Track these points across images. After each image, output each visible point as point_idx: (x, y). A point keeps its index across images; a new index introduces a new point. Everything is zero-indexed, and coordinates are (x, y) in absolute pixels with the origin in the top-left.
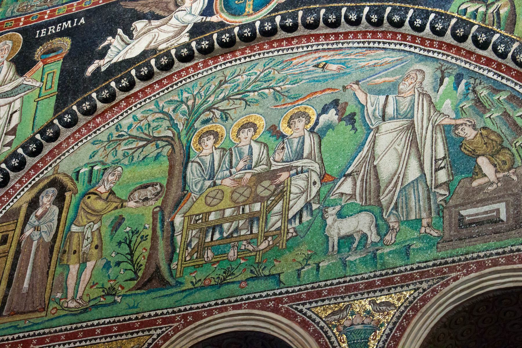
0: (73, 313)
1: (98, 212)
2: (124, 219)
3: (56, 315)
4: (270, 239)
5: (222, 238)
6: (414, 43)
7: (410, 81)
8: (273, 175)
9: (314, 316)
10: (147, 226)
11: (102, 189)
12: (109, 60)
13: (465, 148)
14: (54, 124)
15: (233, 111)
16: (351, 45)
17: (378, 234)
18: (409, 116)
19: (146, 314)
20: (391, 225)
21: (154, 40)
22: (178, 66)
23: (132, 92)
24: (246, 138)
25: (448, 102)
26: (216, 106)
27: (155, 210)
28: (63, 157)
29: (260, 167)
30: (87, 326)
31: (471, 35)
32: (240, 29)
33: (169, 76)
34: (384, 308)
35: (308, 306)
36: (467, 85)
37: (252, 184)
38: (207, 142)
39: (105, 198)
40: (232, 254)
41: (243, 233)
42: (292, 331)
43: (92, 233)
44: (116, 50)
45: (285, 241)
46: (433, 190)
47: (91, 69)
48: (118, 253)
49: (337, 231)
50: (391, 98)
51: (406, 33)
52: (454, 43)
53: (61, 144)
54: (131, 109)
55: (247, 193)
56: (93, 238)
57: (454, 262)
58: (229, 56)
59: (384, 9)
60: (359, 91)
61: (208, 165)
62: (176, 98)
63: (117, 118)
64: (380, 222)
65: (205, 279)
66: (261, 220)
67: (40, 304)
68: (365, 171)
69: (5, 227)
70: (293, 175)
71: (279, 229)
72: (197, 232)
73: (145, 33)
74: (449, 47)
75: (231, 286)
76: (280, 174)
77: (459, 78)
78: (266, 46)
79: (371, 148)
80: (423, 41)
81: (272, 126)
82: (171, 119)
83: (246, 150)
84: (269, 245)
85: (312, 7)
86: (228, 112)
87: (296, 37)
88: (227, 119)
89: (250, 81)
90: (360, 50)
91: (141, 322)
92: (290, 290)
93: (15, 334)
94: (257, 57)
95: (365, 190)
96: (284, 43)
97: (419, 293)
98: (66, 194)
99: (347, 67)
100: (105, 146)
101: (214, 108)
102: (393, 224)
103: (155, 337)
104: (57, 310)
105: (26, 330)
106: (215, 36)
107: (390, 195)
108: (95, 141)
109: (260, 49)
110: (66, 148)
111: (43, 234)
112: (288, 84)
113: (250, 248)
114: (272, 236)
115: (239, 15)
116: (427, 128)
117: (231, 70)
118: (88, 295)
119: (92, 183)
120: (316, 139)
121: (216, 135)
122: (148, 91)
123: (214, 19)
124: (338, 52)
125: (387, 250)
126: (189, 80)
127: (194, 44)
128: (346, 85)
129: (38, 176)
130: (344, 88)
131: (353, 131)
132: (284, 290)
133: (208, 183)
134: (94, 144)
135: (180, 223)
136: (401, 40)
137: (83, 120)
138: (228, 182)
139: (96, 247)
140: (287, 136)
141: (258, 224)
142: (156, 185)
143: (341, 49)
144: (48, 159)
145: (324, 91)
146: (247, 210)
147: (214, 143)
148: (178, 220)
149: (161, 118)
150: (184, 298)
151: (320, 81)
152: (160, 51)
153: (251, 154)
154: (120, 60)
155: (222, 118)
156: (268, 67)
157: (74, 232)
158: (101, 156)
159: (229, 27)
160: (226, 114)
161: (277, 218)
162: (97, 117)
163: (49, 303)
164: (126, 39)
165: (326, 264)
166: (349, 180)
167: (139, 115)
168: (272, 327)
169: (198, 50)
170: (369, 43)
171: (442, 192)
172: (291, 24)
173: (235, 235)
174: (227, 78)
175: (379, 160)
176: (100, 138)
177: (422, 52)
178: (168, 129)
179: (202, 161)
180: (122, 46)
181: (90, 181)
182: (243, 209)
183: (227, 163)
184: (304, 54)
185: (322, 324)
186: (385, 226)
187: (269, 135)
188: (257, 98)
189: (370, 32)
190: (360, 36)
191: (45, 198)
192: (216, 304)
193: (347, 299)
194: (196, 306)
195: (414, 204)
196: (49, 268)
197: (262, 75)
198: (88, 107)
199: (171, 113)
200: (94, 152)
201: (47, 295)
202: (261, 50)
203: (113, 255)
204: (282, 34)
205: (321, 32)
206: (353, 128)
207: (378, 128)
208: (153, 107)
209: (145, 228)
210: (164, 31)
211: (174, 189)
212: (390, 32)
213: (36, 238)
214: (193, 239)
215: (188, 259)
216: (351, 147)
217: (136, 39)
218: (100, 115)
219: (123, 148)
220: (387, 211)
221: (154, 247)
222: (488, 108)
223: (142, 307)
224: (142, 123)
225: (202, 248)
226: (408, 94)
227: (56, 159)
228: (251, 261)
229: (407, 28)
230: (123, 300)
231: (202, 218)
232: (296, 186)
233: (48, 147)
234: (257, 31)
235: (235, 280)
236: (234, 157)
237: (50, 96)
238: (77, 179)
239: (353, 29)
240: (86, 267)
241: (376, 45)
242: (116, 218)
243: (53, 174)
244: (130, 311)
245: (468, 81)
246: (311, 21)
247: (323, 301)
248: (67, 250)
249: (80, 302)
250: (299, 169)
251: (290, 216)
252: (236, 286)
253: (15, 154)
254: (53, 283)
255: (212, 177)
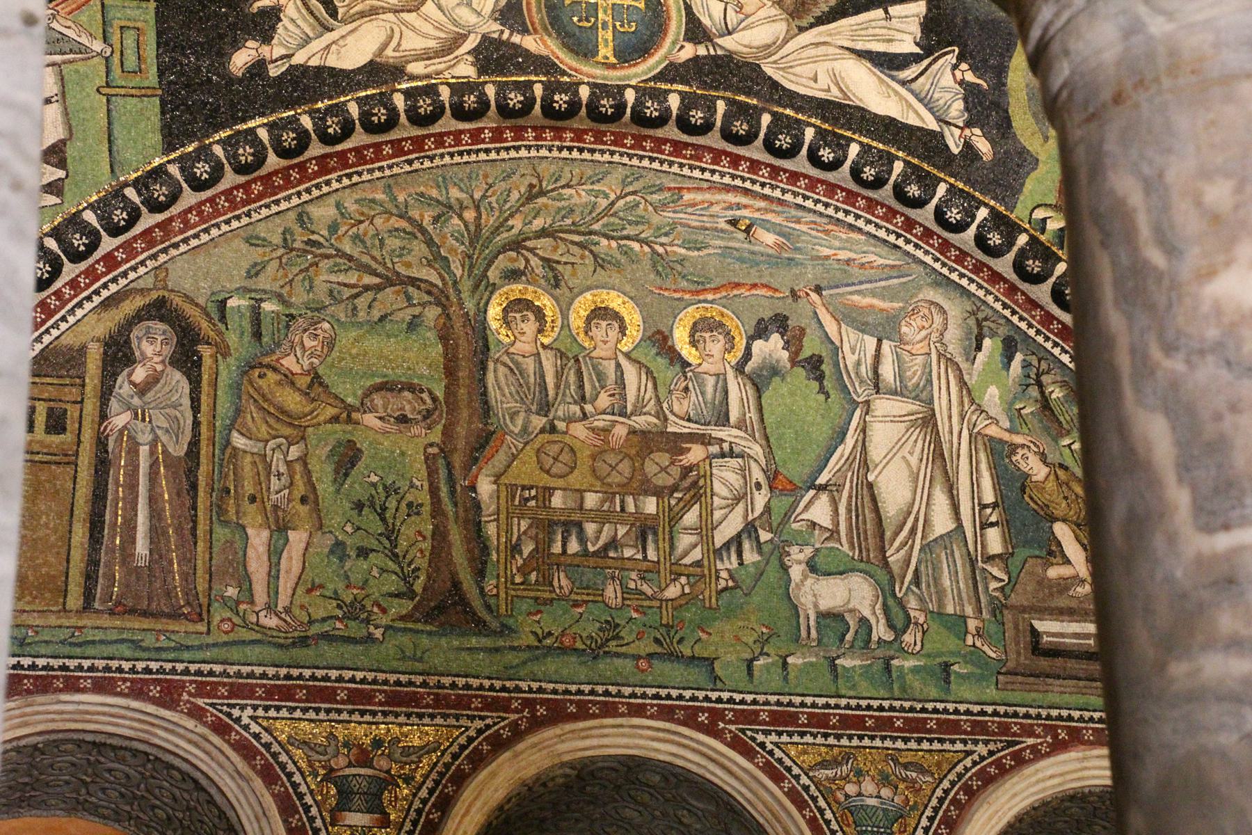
0: (266, 638)
1: (289, 416)
2: (360, 450)
3: (232, 637)
4: (683, 580)
5: (586, 553)
6: (927, 243)
7: (919, 322)
8: (676, 444)
9: (788, 762)
10: (418, 483)
11: (289, 363)
12: (283, 52)
13: (1031, 498)
14: (167, 173)
15: (569, 267)
16: (799, 200)
17: (891, 625)
18: (923, 394)
19: (447, 681)
20: (912, 614)
21: (393, 44)
22: (447, 123)
23: (339, 148)
24: (605, 342)
25: (993, 391)
26: (529, 244)
27: (430, 450)
28: (173, 252)
29: (643, 418)
30: (313, 678)
31: (1053, 279)
32: (592, 94)
33: (418, 137)
34: (914, 775)
35: (774, 738)
36: (1026, 365)
37: (633, 452)
38: (523, 325)
39: (304, 387)
40: (611, 593)
41: (628, 553)
42: (754, 785)
43: (289, 464)
44: (298, 31)
45: (714, 593)
46: (980, 564)
47: (240, 60)
48: (359, 528)
49: (810, 598)
50: (886, 346)
51: (918, 220)
52: (1012, 276)
53: (171, 219)
54: (328, 183)
55: (625, 467)
56: (291, 477)
57: (1027, 716)
58: (548, 134)
59: (891, 159)
60: (824, 310)
61: (532, 380)
62: (434, 193)
63: (299, 194)
64: (891, 602)
65: (563, 634)
66: (661, 536)
67: (188, 603)
68: (851, 487)
69: (50, 388)
70: (715, 457)
71: (698, 564)
72: (530, 526)
73: (362, 15)
74: (996, 277)
75: (618, 662)
76: (688, 445)
77: (1009, 348)
78: (629, 142)
79: (860, 444)
80: (945, 246)
81: (659, 332)
82: (430, 242)
83: (610, 368)
84: (684, 594)
85: (742, 98)
86: (560, 268)
87: (693, 145)
88: (557, 286)
89: (598, 211)
90: (818, 220)
91: (437, 695)
92: (738, 697)
93: (137, 660)
94: (607, 157)
95: (856, 532)
96: (667, 148)
97: (975, 763)
98: (200, 348)
99: (797, 249)
100: (280, 258)
101: (529, 250)
102: (917, 614)
103: (472, 733)
104: (234, 625)
105: (164, 656)
106: (538, 90)
107: (902, 552)
108: (251, 237)
109: (614, 143)
110: (182, 232)
111: (159, 432)
112: (679, 246)
113: (645, 588)
114: (688, 576)
115: (585, 55)
116: (960, 433)
117: (553, 168)
118: (302, 607)
119: (265, 340)
120: (751, 392)
121: (539, 314)
122: (369, 154)
123: (530, 43)
124: (774, 207)
125: (910, 663)
126: (457, 159)
127: (490, 91)
128: (796, 288)
129: (114, 280)
130: (794, 294)
131: (822, 397)
132: (725, 695)
133: (538, 422)
134: (252, 245)
135: (491, 497)
136: (901, 228)
137: (230, 179)
138: (579, 430)
139: (304, 500)
140: (689, 365)
141: (656, 542)
142: (422, 391)
143: (781, 202)
144: (138, 245)
145: (754, 286)
146: (631, 508)
147: (540, 331)
148: (485, 487)
149: (404, 231)
150: (524, 663)
151: (741, 260)
152: (412, 78)
153: (621, 382)
154: (312, 63)
155: (548, 280)
156: (631, 189)
157: (245, 452)
158: (275, 280)
159: (566, 79)
160: (553, 269)
161: (693, 539)
162: (255, 181)
163: (209, 605)
164: (319, 10)
165: (800, 661)
166: (824, 498)
167: (351, 207)
168: (711, 766)
169: (499, 107)
170: (837, 209)
171: (996, 572)
172: (699, 122)
173: (612, 554)
174: (544, 184)
175: (876, 472)
176: (261, 230)
177: (937, 266)
178: (430, 265)
179: (517, 364)
180: (313, 29)
181: (257, 335)
182: (622, 501)
183: (572, 387)
184: (705, 185)
185: (804, 780)
186: (901, 615)
187: (654, 351)
188: (619, 257)
189: (843, 189)
190: (820, 188)
191: (145, 344)
192: (592, 692)
193: (844, 742)
194: (551, 686)
195: (948, 583)
196: (195, 522)
197: (621, 203)
198: (250, 158)
199: (430, 228)
200: (256, 264)
201: (201, 586)
202: (616, 145)
203: (349, 529)
204: (671, 131)
205: (747, 155)
206: (822, 390)
207: (867, 403)
208: (380, 196)
209: (412, 486)
210: (414, 29)
211: (465, 414)
212: (883, 205)
213: (145, 438)
214: (523, 537)
215: (518, 579)
216: (821, 432)
217: (344, 22)
218: (261, 178)
219: (325, 277)
220: (902, 583)
221: (440, 535)
222: (1065, 426)
223: (438, 661)
224: (362, 226)
225: (543, 562)
226: (920, 348)
227: (155, 250)
228: (652, 618)
229: (926, 216)
230: (387, 635)
231: (533, 498)
232: (724, 483)
233: (148, 220)
234: (629, 110)
235: (624, 649)
236: (585, 379)
237: (143, 93)
238: (223, 318)
239: (815, 172)
240: (288, 540)
241: (850, 219)
242: (339, 443)
243: (155, 288)
244: (409, 665)
245: (1028, 358)
246: (741, 132)
247: (802, 734)
248: (232, 488)
249: (288, 619)
250: (726, 446)
251: (718, 544)
252: (629, 663)
253: (75, 221)
254: (211, 559)
255: (545, 407)
